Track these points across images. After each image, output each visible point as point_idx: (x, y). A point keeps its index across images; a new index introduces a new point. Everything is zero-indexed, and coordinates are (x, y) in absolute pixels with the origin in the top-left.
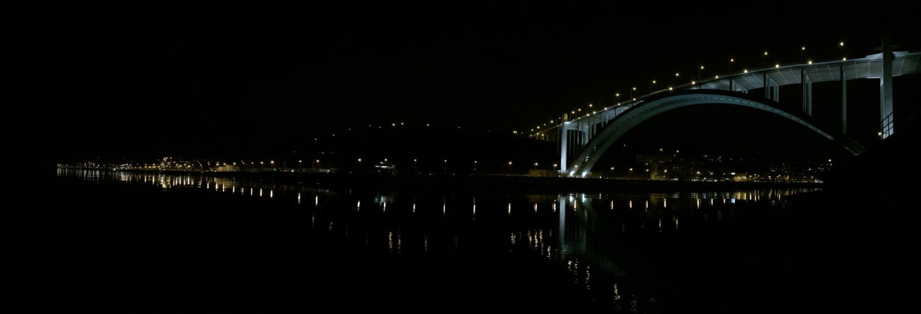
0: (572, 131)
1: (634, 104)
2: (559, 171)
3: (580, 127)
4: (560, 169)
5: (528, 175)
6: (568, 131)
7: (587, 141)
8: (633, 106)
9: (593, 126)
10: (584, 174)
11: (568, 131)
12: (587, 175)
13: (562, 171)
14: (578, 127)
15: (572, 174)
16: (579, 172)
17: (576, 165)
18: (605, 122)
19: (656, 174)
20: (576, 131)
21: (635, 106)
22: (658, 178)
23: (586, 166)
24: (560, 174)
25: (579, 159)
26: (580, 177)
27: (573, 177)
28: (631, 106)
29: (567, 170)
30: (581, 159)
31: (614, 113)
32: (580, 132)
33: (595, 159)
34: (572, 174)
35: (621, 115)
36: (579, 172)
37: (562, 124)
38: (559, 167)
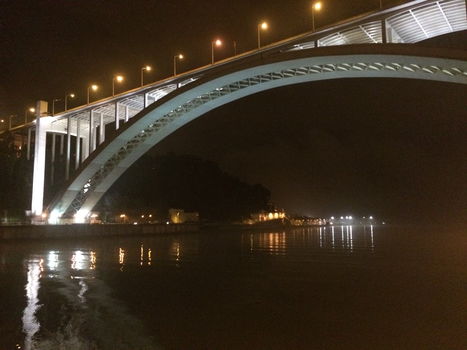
0: (58, 136)
1: (180, 85)
6: (49, 136)
7: (86, 155)
8: (178, 89)
9: (98, 129)
18: (121, 122)
20: (66, 136)
21: (182, 87)
23: (83, 202)
25: (70, 189)
28: (173, 88)
30: (75, 187)
32: (74, 139)
33: (103, 188)
37: (35, 121)
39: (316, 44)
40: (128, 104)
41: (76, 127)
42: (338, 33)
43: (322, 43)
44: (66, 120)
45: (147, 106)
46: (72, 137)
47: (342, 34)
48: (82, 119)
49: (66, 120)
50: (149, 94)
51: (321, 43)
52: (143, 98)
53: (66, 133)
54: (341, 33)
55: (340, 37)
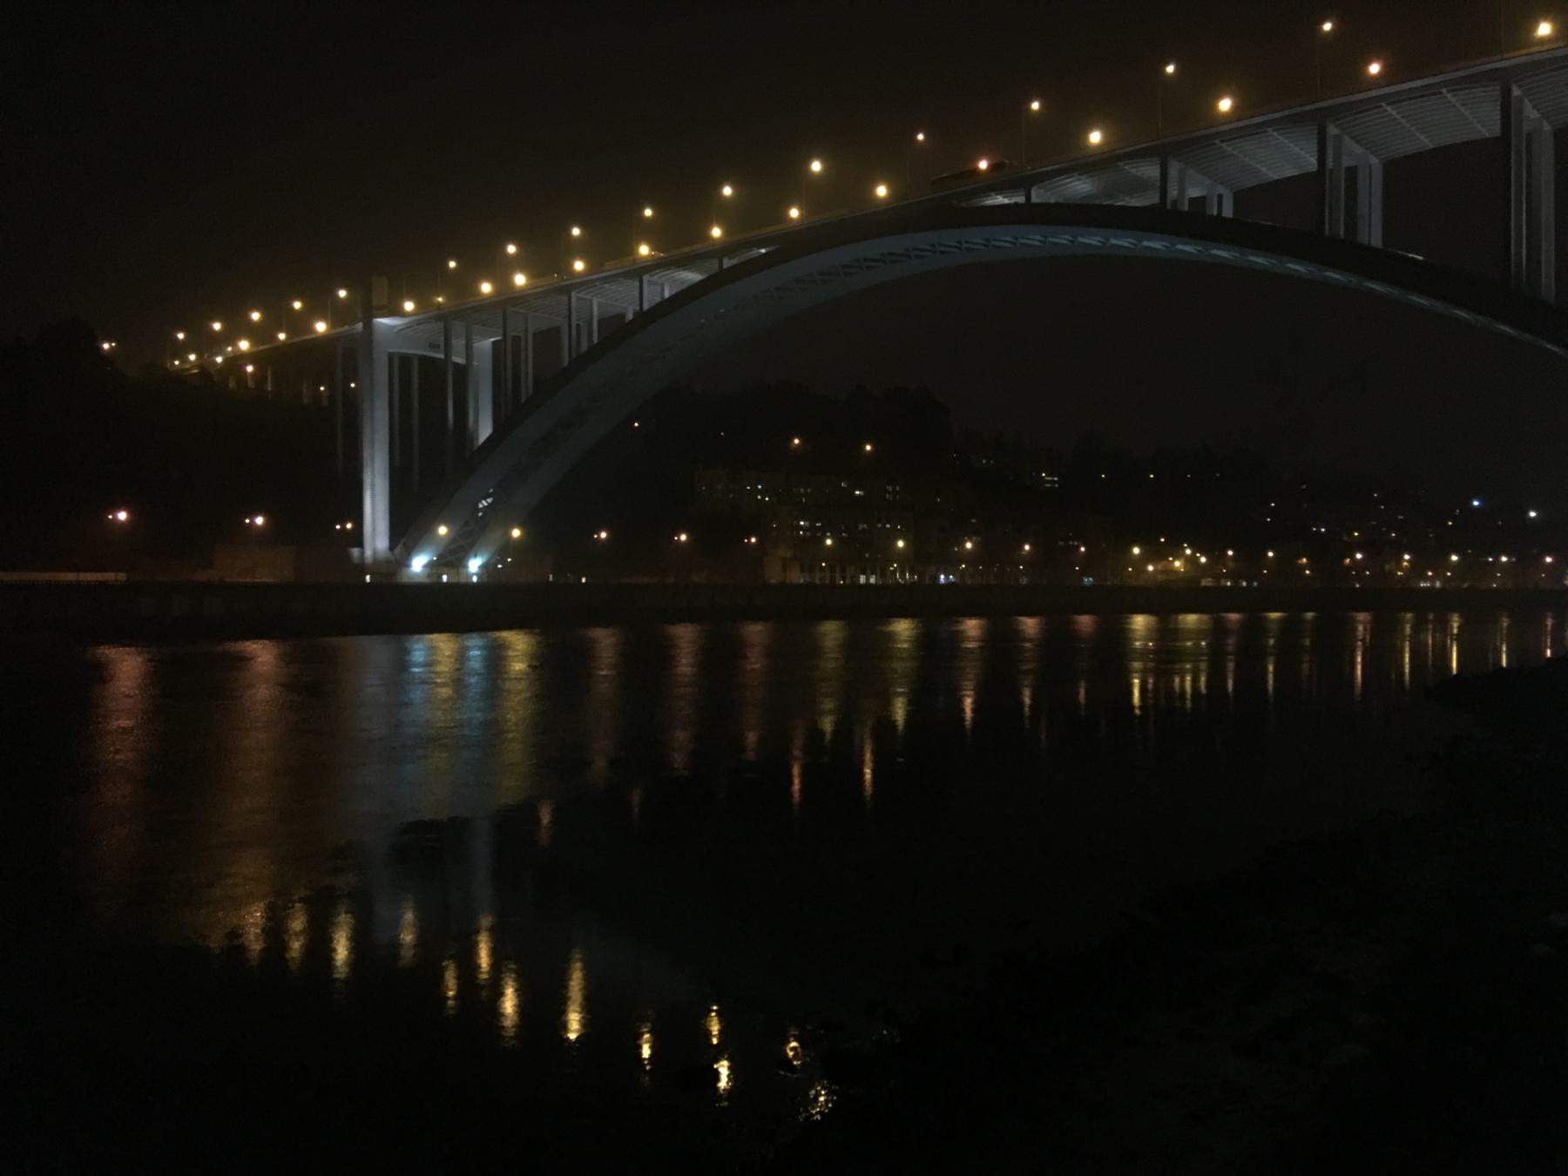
1: (727, 263)
2: (355, 551)
3: (458, 343)
4: (360, 543)
5: (202, 576)
10: (474, 565)
11: (391, 356)
13: (368, 553)
15: (419, 563)
16: (452, 557)
17: (446, 523)
19: (789, 554)
22: (797, 577)
24: (362, 568)
26: (454, 580)
27: (426, 580)
28: (713, 266)
29: (392, 547)
34: (419, 563)
35: (667, 307)
36: (452, 557)
38: (357, 538)
39: (1028, 197)
40: (596, 295)
42: (1076, 174)
43: (1042, 191)
44: (441, 325)
45: (646, 307)
46: (456, 365)
47: (1086, 175)
48: (477, 324)
49: (441, 325)
50: (651, 276)
52: (637, 284)
53: (442, 356)
54: (1080, 174)
55: (1080, 180)
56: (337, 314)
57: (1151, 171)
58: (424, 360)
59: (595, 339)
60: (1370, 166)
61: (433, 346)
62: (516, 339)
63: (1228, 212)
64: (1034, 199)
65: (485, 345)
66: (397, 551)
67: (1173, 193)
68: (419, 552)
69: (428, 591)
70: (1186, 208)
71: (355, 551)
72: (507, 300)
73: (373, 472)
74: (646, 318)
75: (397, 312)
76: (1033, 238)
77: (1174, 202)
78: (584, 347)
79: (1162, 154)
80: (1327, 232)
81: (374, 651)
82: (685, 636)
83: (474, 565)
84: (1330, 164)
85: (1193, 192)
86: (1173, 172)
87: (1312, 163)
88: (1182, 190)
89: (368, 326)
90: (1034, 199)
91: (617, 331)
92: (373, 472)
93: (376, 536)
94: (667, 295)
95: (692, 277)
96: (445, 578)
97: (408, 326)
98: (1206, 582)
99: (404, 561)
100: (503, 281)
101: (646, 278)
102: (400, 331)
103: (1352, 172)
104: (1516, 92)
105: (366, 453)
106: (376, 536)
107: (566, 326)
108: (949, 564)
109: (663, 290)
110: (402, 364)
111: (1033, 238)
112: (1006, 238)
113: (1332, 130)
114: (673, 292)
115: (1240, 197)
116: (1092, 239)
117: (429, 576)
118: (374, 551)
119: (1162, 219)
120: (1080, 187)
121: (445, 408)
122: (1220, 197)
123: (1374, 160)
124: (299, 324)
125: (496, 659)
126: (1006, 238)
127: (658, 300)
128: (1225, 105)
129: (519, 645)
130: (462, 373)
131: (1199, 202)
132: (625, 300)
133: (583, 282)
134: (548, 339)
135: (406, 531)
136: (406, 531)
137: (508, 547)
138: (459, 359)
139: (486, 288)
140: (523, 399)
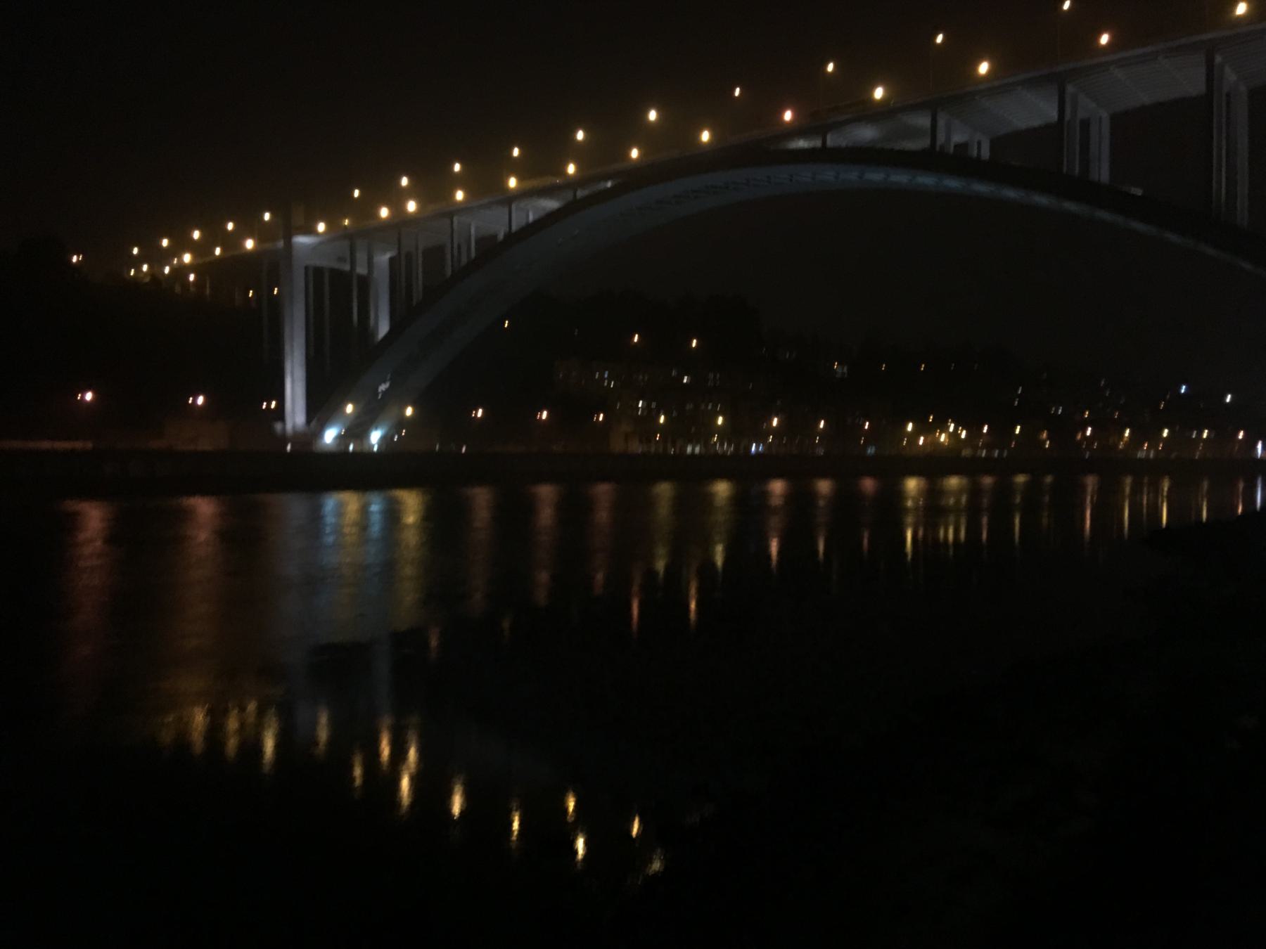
1: (580, 194)
3: (361, 257)
10: (375, 437)
11: (306, 268)
12: (384, 440)
13: (289, 426)
14: (353, 263)
15: (330, 435)
16: (357, 430)
22: (636, 447)
24: (284, 439)
26: (359, 449)
28: (569, 196)
31: (507, 217)
34: (330, 435)
35: (531, 229)
36: (357, 430)
38: (280, 413)
39: (824, 142)
41: (366, 258)
45: (514, 228)
51: (831, 140)
56: (262, 233)
57: (923, 121)
58: (332, 271)
59: (473, 255)
60: (1100, 118)
61: (341, 259)
62: (409, 256)
63: (986, 153)
64: (830, 143)
65: (383, 259)
66: (313, 423)
67: (941, 138)
68: (330, 426)
69: (337, 457)
70: (952, 150)
71: (278, 426)
72: (401, 221)
73: (292, 361)
74: (514, 238)
75: (311, 231)
76: (828, 175)
77: (942, 147)
78: (464, 260)
79: (933, 107)
80: (1065, 170)
81: (293, 506)
82: (546, 493)
83: (375, 437)
84: (1068, 116)
85: (957, 138)
86: (941, 123)
87: (1054, 115)
88: (948, 138)
89: (289, 244)
90: (830, 143)
91: (490, 248)
92: (292, 361)
93: (296, 414)
94: (531, 218)
95: (551, 204)
96: (351, 447)
97: (321, 243)
98: (966, 452)
99: (319, 433)
100: (398, 208)
101: (514, 206)
102: (314, 248)
103: (1085, 124)
104: (1218, 59)
105: (287, 348)
106: (296, 414)
107: (449, 246)
108: (760, 438)
109: (528, 216)
110: (316, 274)
111: (828, 175)
112: (806, 175)
113: (1070, 89)
114: (537, 217)
115: (996, 143)
116: (876, 176)
117: (339, 445)
118: (294, 427)
119: (931, 159)
120: (866, 134)
121: (351, 309)
122: (979, 143)
123: (1105, 115)
124: (232, 242)
125: (393, 515)
126: (806, 175)
127: (523, 223)
128: (984, 68)
129: (412, 504)
130: (365, 283)
131: (962, 147)
132: (496, 223)
133: (462, 209)
134: (434, 254)
135: (319, 409)
136: (319, 409)
137: (402, 422)
138: (361, 270)
139: (384, 212)
140: (414, 302)
